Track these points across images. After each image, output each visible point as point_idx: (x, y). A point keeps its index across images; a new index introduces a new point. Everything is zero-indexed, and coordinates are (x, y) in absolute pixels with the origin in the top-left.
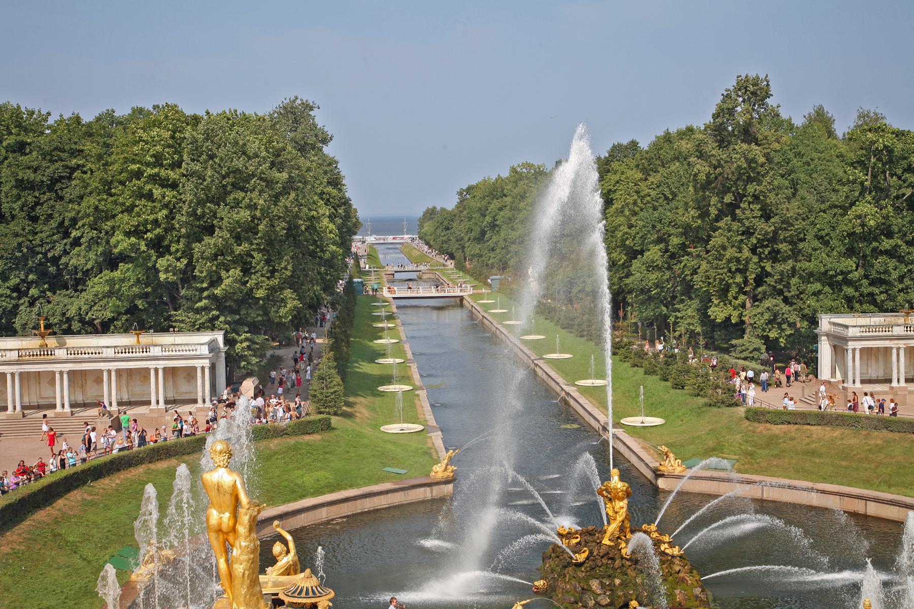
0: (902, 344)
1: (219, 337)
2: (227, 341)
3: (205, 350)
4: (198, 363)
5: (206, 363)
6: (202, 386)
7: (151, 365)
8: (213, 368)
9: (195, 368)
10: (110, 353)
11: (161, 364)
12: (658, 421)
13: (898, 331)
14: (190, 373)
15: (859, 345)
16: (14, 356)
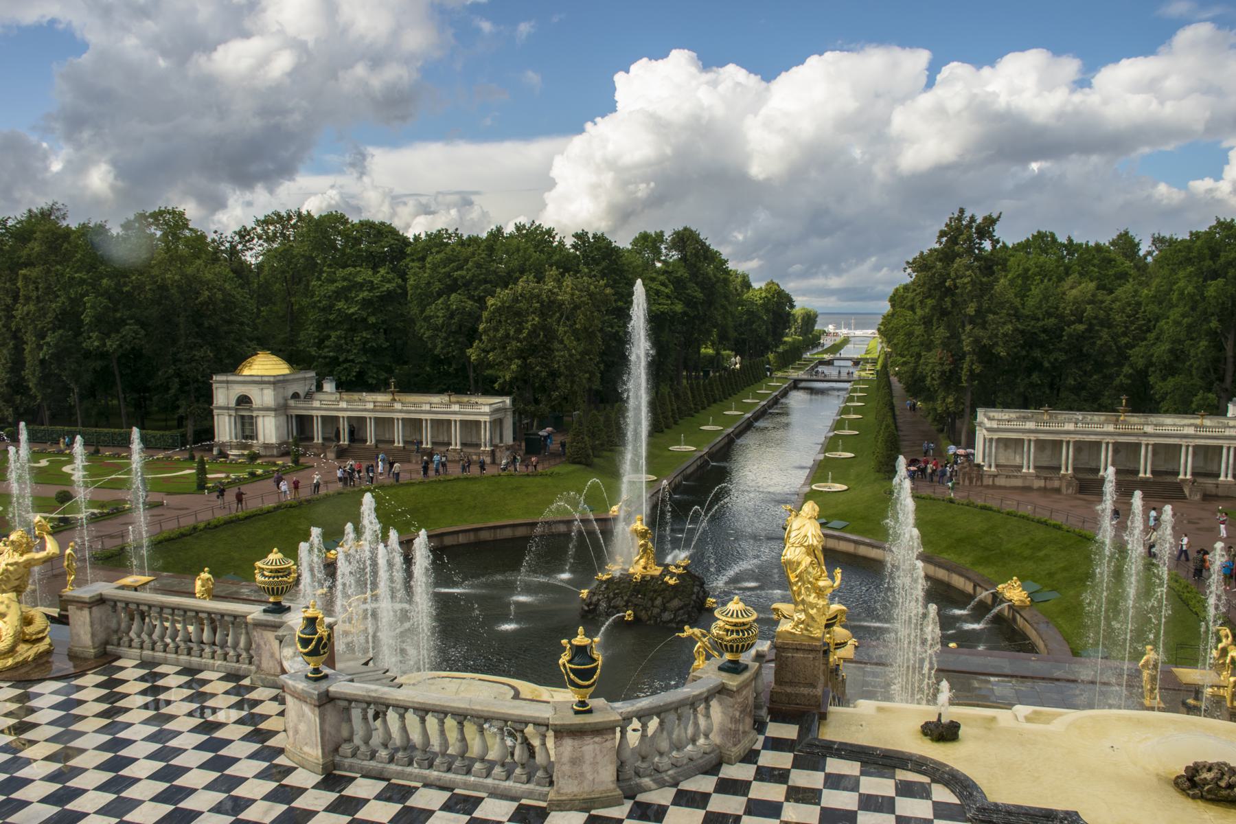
0: (1033, 437)
1: (508, 400)
2: (514, 402)
3: (487, 409)
4: (482, 419)
5: (487, 418)
6: (485, 435)
7: (452, 417)
8: (497, 424)
9: (479, 422)
10: (427, 407)
11: (459, 417)
12: (845, 487)
13: (1030, 425)
14: (478, 423)
15: (996, 436)
16: (371, 406)
